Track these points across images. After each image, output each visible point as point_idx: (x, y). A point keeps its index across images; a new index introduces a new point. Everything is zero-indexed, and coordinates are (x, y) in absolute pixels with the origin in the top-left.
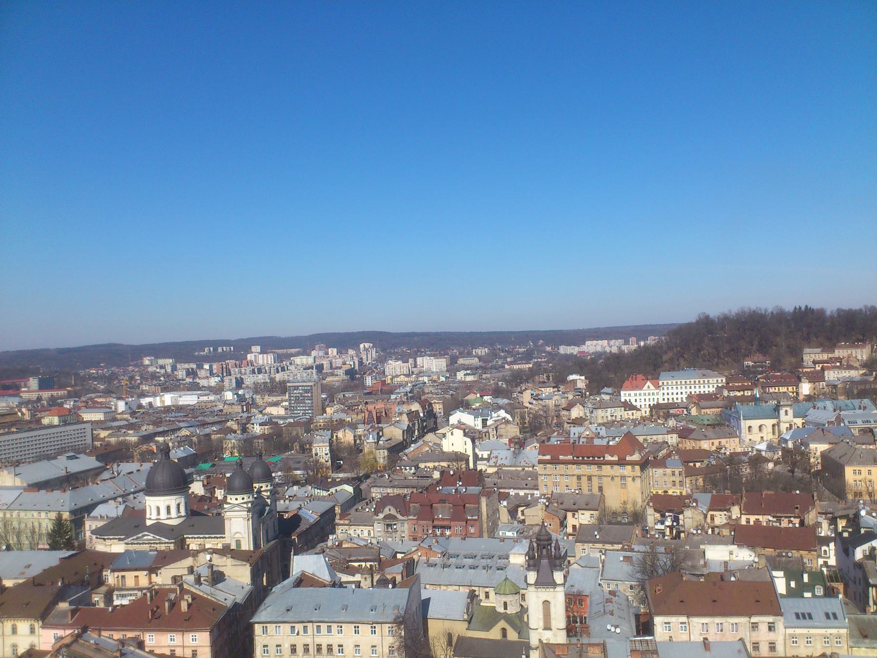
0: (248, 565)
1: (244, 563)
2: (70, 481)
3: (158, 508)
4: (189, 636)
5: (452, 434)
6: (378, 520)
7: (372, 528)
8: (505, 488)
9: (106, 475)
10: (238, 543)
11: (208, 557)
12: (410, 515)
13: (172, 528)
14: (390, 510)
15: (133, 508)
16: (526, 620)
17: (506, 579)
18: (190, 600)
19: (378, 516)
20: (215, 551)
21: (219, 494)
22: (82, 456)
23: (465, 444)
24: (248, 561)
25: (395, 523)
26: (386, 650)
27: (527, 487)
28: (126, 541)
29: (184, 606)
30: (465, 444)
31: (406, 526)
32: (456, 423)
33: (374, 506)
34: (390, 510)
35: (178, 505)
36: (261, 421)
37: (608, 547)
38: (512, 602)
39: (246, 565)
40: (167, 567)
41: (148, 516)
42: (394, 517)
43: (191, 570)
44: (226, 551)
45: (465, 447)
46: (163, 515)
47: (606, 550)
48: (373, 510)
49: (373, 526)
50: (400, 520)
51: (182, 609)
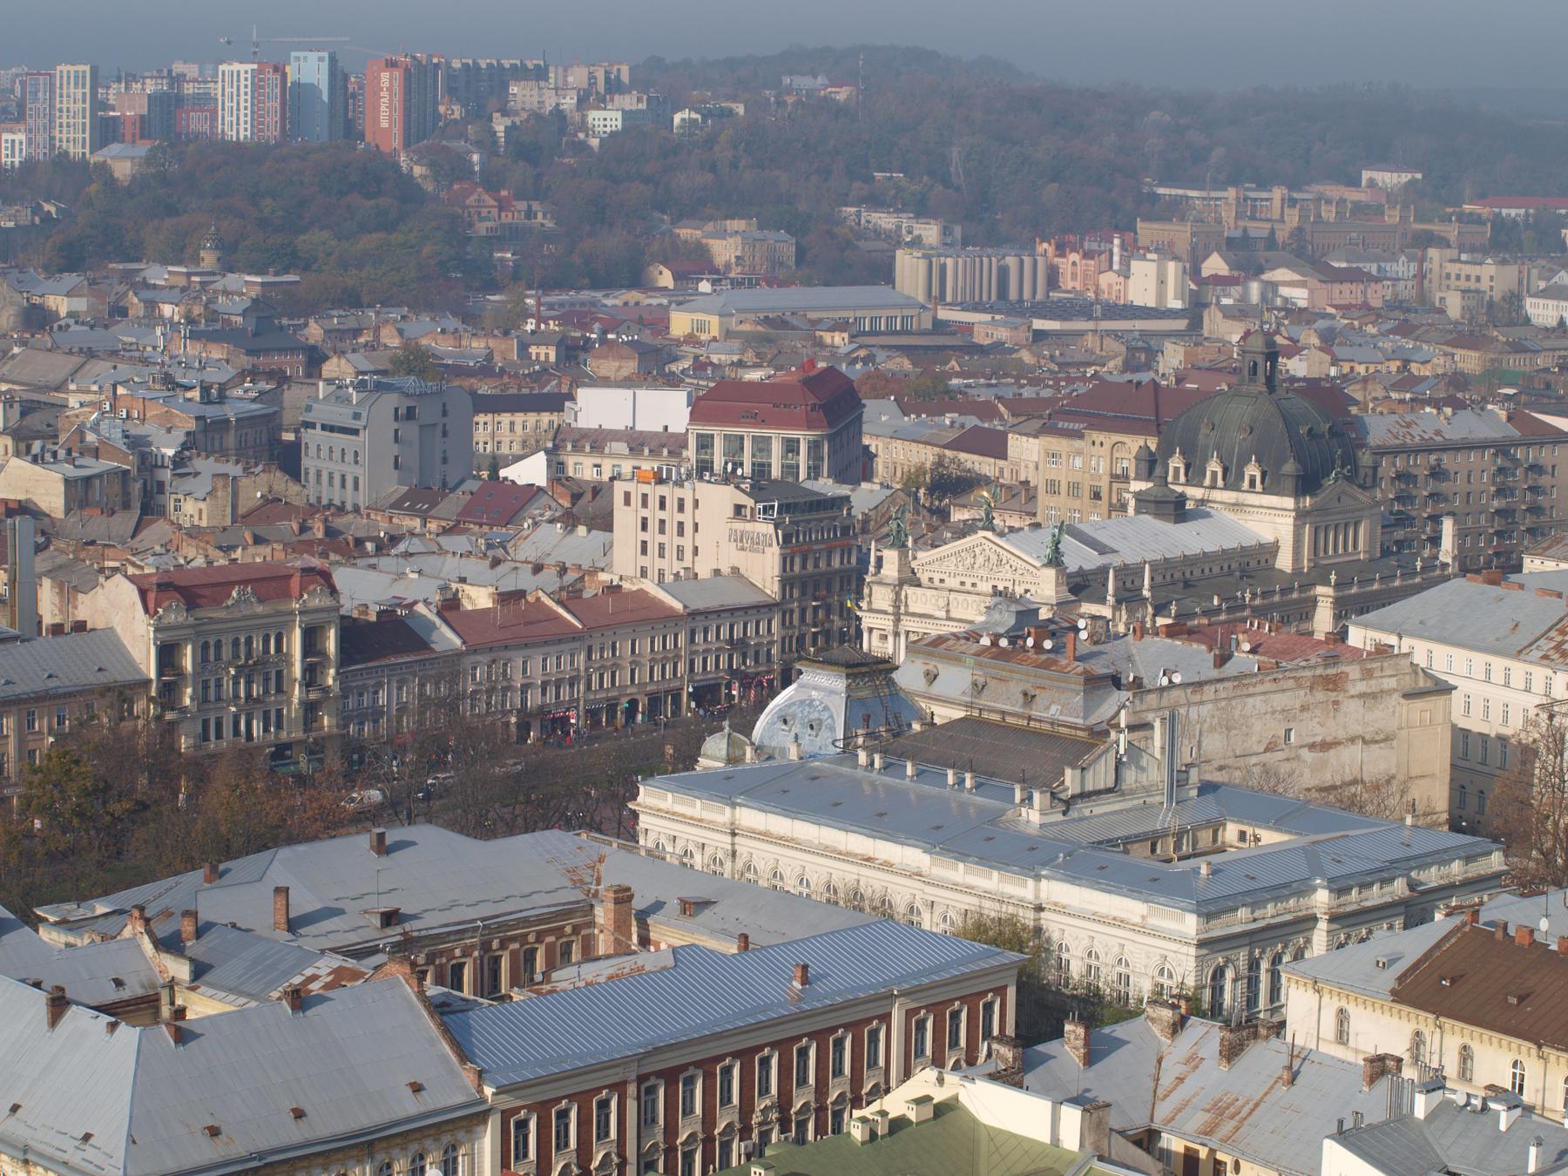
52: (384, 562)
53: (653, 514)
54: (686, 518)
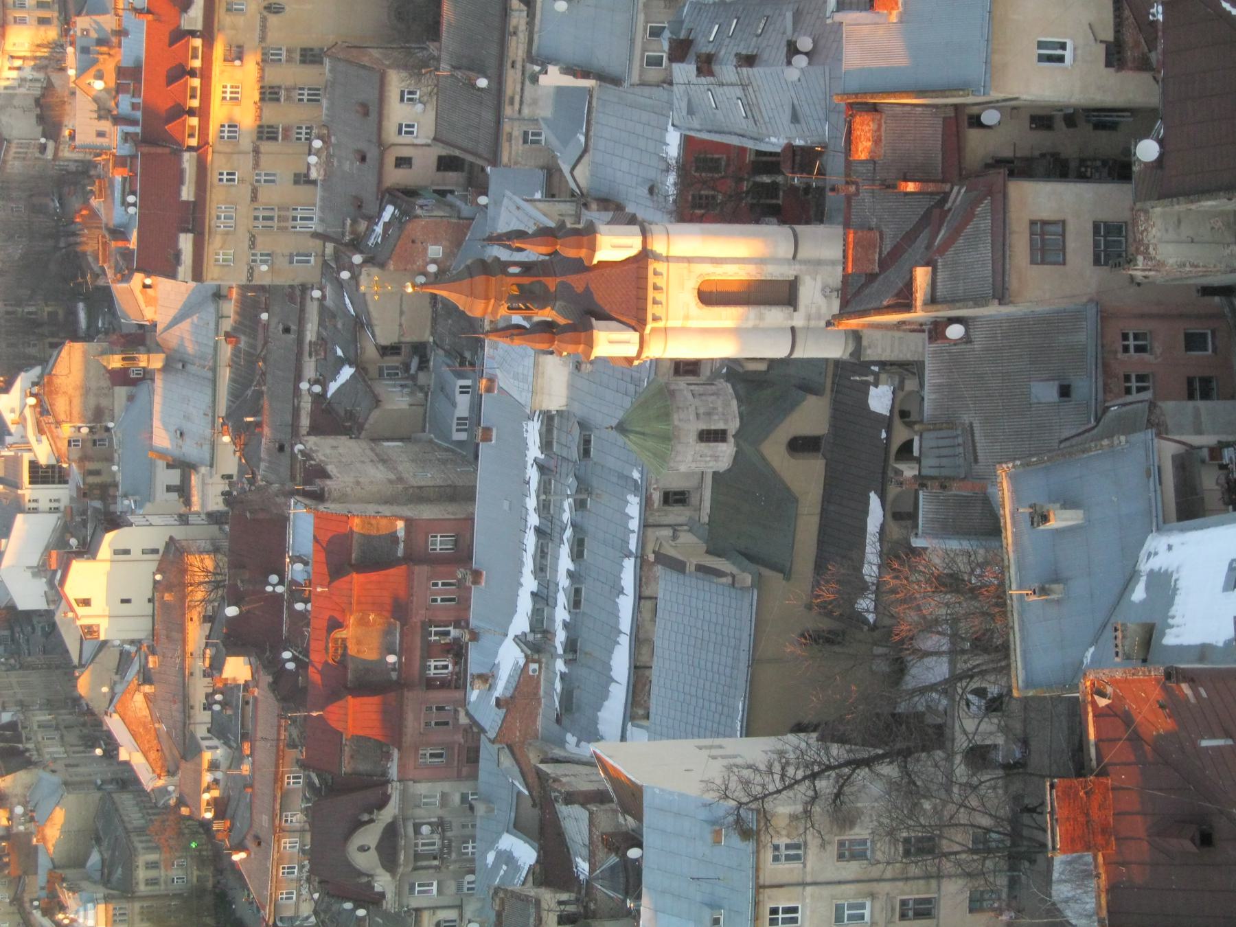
5: (86, 602)
6: (399, 893)
7: (426, 916)
8: (296, 412)
12: (384, 773)
14: (363, 849)
16: (762, 367)
17: (621, 428)
19: (382, 895)
23: (127, 552)
25: (411, 830)
26: (852, 869)
27: (294, 328)
30: (127, 552)
31: (422, 788)
32: (41, 585)
33: (348, 906)
34: (363, 849)
37: (517, 48)
38: (701, 411)
42: (391, 833)
45: (136, 553)
47: (530, 58)
48: (361, 912)
49: (418, 910)
50: (402, 809)
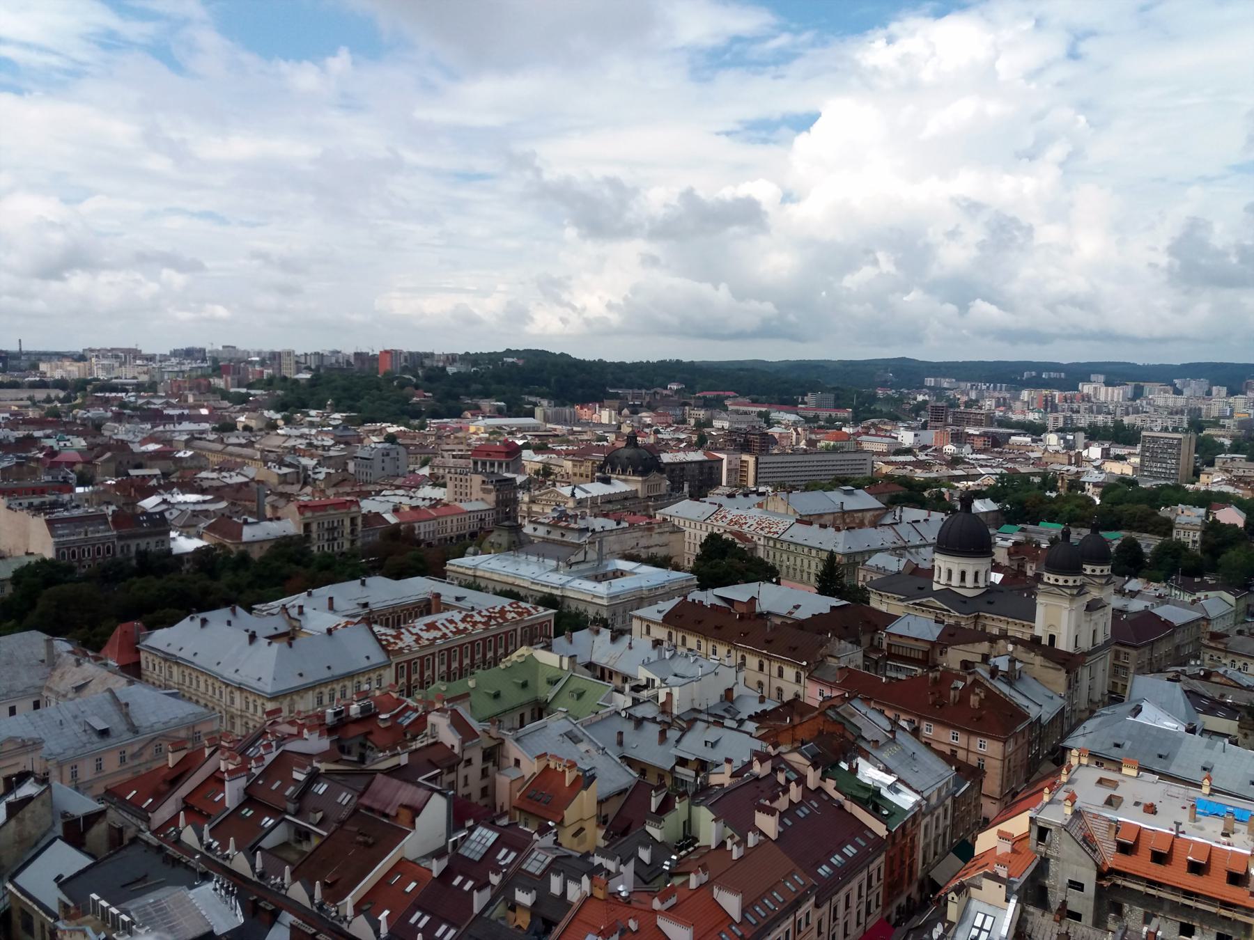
0: (1063, 671)
1: (1059, 667)
2: (846, 521)
3: (950, 572)
4: (975, 742)
9: (888, 520)
10: (1052, 638)
11: (1010, 647)
13: (964, 600)
15: (917, 565)
18: (982, 695)
20: (1016, 642)
21: (1030, 570)
22: (860, 492)
24: (1063, 665)
28: (906, 603)
29: (974, 700)
35: (976, 574)
36: (1095, 480)
39: (1060, 670)
40: (957, 647)
41: (936, 579)
43: (985, 658)
44: (1034, 643)
46: (955, 581)
51: (971, 704)
52: (378, 498)
53: (458, 483)
54: (468, 484)
